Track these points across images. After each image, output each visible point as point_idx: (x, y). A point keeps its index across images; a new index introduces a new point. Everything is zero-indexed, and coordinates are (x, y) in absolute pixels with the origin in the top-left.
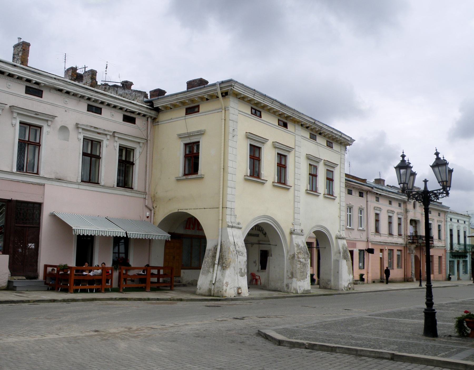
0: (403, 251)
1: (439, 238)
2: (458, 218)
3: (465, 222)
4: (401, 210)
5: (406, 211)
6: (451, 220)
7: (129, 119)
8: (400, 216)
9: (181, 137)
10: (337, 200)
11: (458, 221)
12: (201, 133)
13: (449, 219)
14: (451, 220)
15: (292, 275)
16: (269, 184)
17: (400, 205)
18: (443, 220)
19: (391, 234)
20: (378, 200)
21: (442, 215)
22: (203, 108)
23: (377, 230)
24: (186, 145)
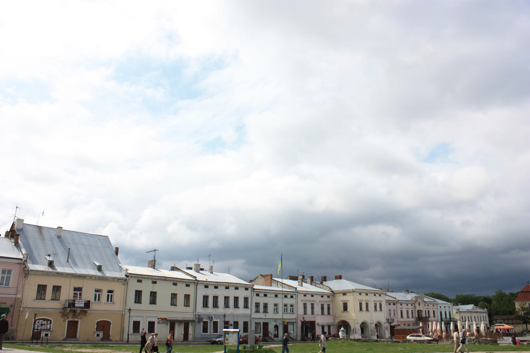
0: (415, 324)
1: (434, 316)
2: (445, 306)
3: (449, 307)
4: (412, 307)
5: (415, 307)
6: (440, 307)
7: (329, 297)
8: (412, 310)
9: (342, 301)
10: (383, 312)
11: (445, 307)
12: (348, 301)
13: (439, 307)
14: (440, 307)
15: (372, 335)
16: (364, 312)
17: (412, 305)
18: (436, 308)
19: (408, 317)
20: (401, 305)
21: (435, 305)
22: (347, 294)
23: (402, 317)
24: (343, 303)
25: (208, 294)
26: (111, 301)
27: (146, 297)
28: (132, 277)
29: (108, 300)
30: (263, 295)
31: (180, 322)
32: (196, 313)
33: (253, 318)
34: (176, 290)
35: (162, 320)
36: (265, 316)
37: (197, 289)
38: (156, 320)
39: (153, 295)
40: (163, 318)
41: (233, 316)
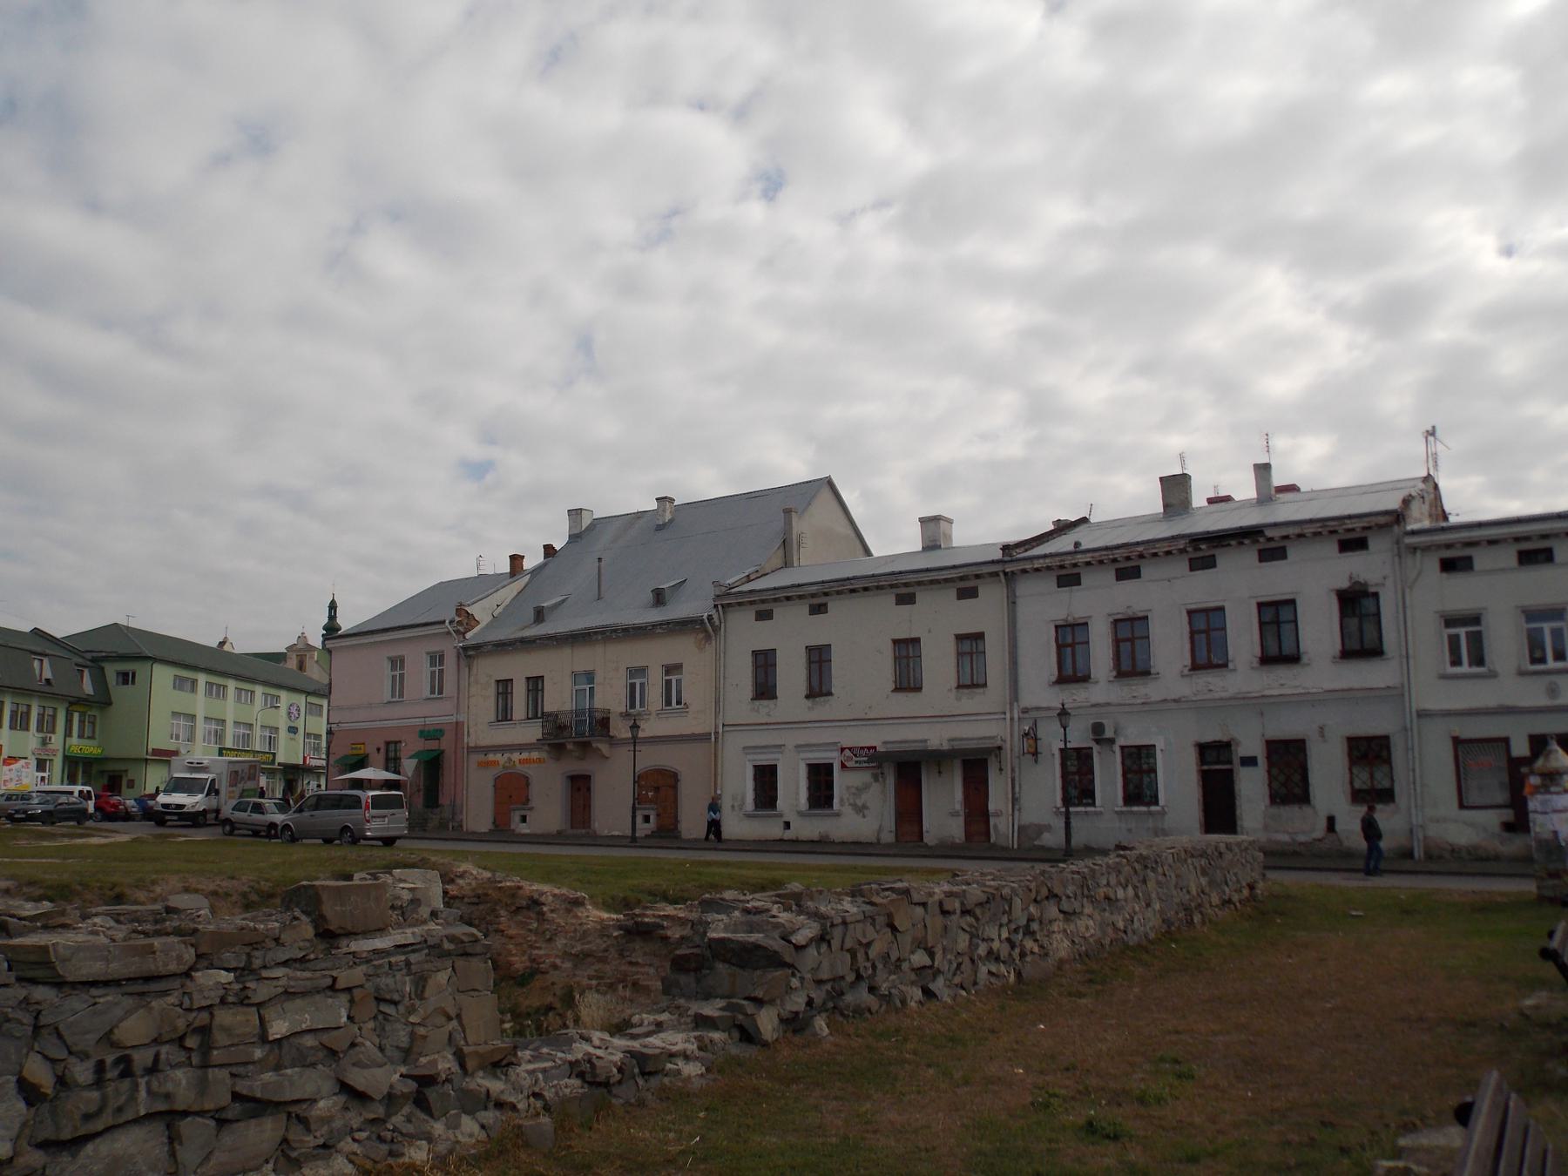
25: (1079, 613)
26: (679, 703)
27: (791, 675)
28: (729, 605)
29: (669, 703)
30: (1513, 561)
31: (939, 759)
32: (1016, 712)
33: (1423, 714)
34: (911, 621)
35: (855, 755)
36: (1553, 691)
37: (1012, 603)
38: (833, 757)
39: (819, 657)
40: (862, 748)
41: (1259, 705)
